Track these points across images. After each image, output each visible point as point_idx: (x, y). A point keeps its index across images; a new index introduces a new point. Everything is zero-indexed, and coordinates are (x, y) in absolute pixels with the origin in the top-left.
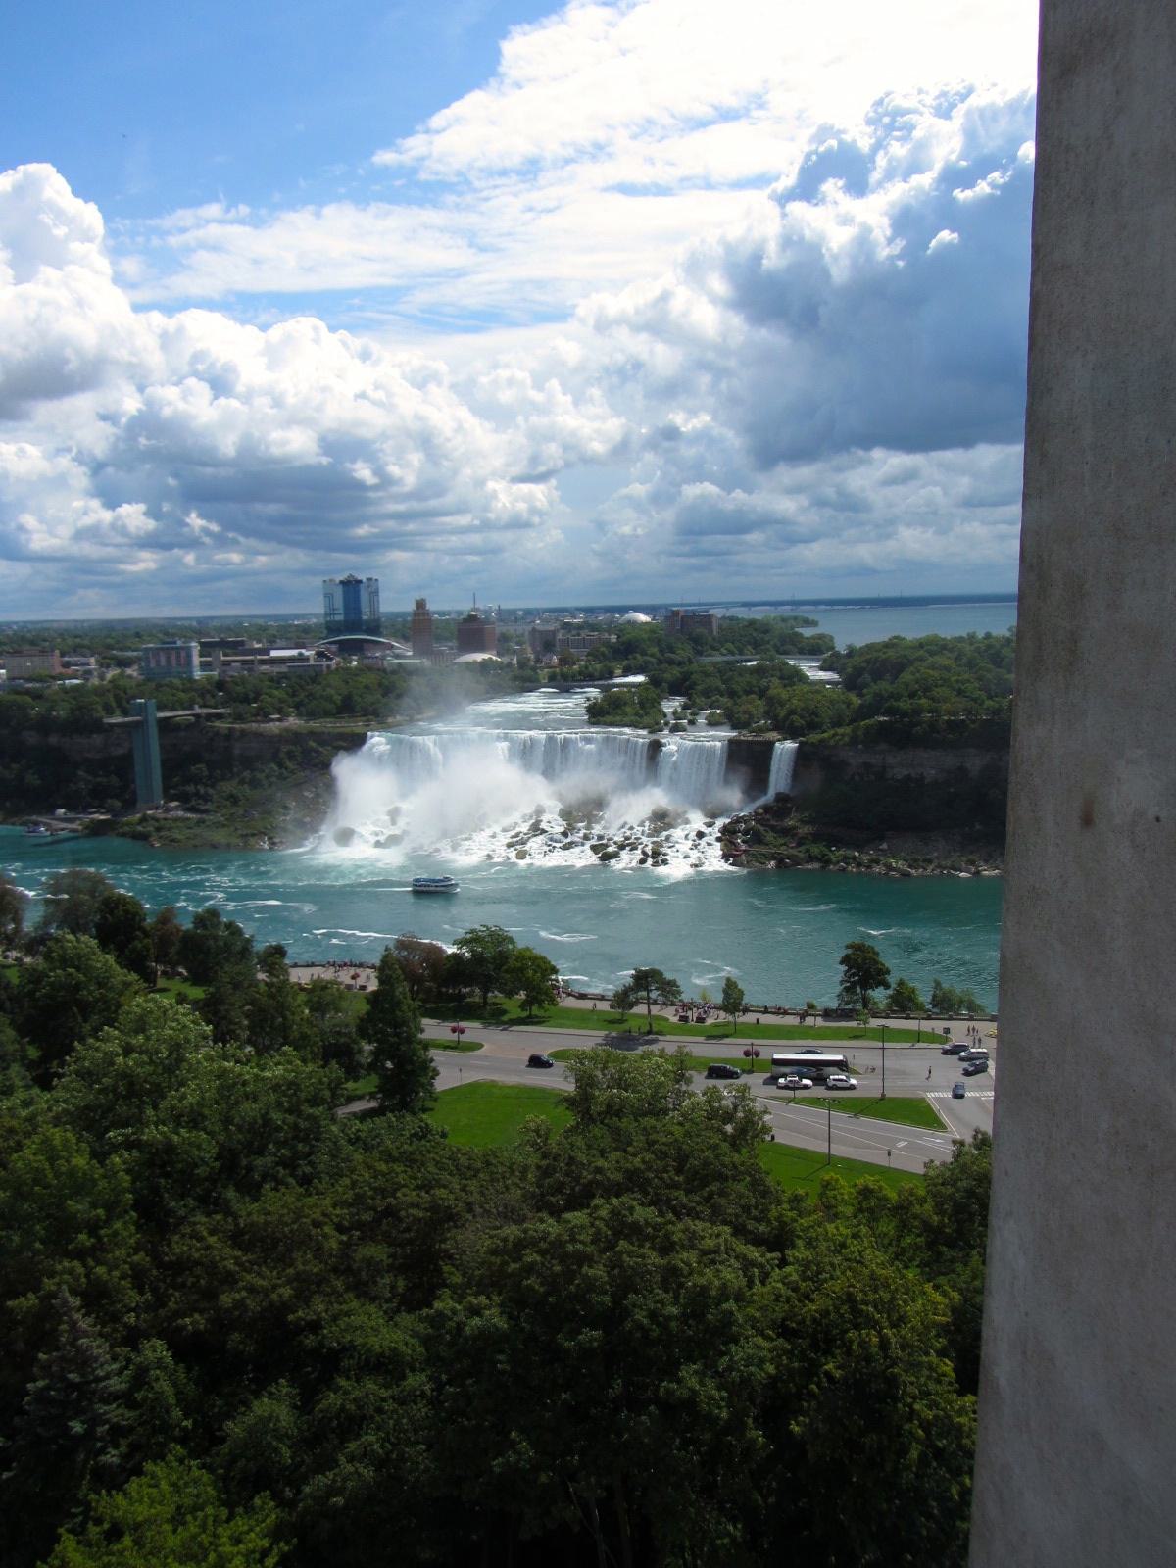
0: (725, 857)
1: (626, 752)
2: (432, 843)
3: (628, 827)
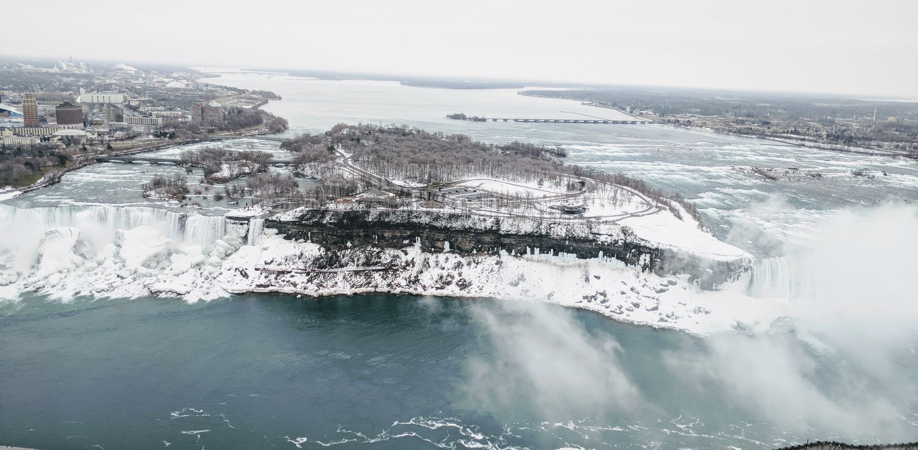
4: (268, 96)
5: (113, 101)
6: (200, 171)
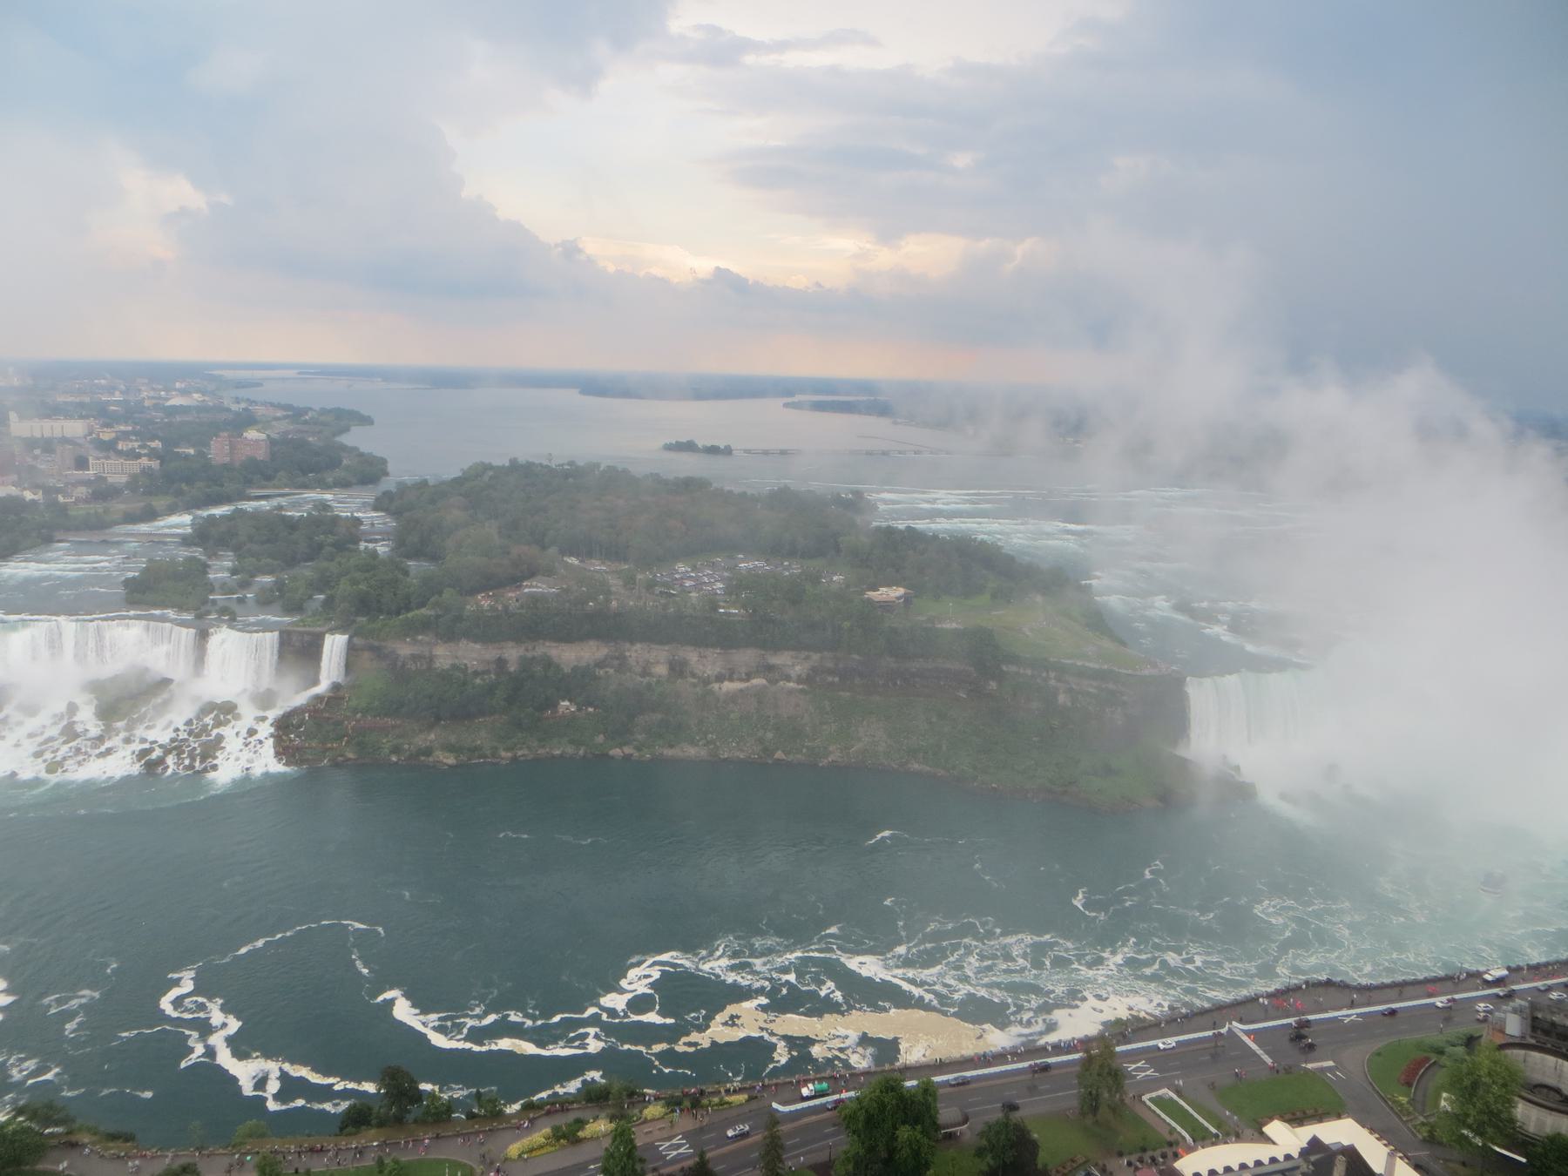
0: (278, 754)
1: (170, 642)
3: (171, 729)
4: (347, 418)
5: (68, 434)
6: (230, 554)
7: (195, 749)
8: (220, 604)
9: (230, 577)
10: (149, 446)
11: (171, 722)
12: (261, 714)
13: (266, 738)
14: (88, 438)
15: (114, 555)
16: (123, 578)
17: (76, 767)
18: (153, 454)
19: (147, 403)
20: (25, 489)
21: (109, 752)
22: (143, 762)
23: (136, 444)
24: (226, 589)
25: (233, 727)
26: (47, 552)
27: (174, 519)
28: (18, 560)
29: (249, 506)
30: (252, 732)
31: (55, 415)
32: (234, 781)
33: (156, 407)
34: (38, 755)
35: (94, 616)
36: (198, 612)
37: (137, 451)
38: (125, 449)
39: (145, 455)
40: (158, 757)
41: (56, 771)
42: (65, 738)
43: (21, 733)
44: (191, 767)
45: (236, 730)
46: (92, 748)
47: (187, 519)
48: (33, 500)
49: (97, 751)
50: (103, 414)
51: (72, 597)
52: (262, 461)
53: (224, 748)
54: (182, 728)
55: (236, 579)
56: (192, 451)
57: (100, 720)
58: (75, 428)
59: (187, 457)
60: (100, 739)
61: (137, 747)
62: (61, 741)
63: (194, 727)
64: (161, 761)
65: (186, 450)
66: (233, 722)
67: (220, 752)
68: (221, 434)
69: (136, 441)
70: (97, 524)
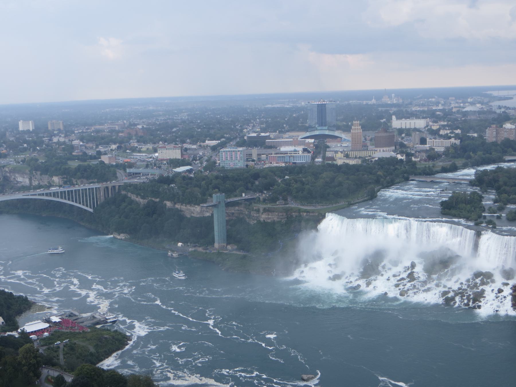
1: (461, 237)
2: (357, 280)
3: (460, 282)
6: (494, 191)
7: (470, 295)
8: (488, 218)
9: (492, 204)
10: (455, 132)
11: (459, 279)
12: (506, 281)
13: (508, 296)
14: (426, 128)
15: (436, 188)
16: (440, 201)
17: (413, 295)
18: (457, 137)
19: (454, 110)
20: (398, 154)
21: (428, 290)
22: (444, 298)
23: (449, 132)
24: (491, 210)
25: (490, 287)
26: (406, 185)
27: (466, 171)
28: (393, 189)
29: (505, 165)
30: (500, 291)
31: (411, 117)
32: (489, 316)
33: (458, 112)
34: (397, 286)
35: (426, 219)
36: (477, 221)
37: (449, 135)
38: (443, 134)
39: (453, 137)
40: (452, 296)
41: (404, 296)
42: (409, 279)
43: (390, 274)
44: (467, 304)
45: (492, 288)
46: (421, 286)
47: (472, 171)
48: (401, 160)
49: (423, 288)
50: (432, 116)
51: (416, 209)
52: (512, 140)
53: (485, 297)
54: (464, 283)
55: (496, 205)
56: (476, 135)
57: (426, 273)
58: (420, 123)
59: (474, 138)
60: (425, 283)
61: (441, 289)
62: (407, 280)
63: (470, 283)
64: (453, 299)
65: (473, 135)
66: (491, 284)
67: (483, 299)
68: (492, 126)
69: (449, 130)
70: (429, 172)
